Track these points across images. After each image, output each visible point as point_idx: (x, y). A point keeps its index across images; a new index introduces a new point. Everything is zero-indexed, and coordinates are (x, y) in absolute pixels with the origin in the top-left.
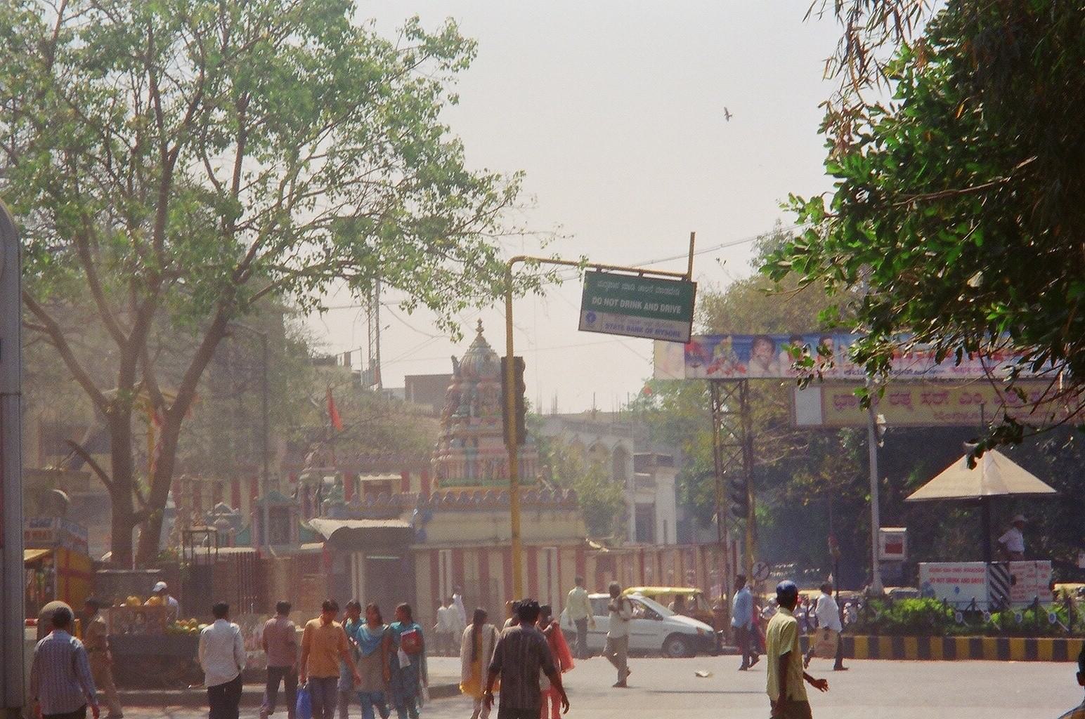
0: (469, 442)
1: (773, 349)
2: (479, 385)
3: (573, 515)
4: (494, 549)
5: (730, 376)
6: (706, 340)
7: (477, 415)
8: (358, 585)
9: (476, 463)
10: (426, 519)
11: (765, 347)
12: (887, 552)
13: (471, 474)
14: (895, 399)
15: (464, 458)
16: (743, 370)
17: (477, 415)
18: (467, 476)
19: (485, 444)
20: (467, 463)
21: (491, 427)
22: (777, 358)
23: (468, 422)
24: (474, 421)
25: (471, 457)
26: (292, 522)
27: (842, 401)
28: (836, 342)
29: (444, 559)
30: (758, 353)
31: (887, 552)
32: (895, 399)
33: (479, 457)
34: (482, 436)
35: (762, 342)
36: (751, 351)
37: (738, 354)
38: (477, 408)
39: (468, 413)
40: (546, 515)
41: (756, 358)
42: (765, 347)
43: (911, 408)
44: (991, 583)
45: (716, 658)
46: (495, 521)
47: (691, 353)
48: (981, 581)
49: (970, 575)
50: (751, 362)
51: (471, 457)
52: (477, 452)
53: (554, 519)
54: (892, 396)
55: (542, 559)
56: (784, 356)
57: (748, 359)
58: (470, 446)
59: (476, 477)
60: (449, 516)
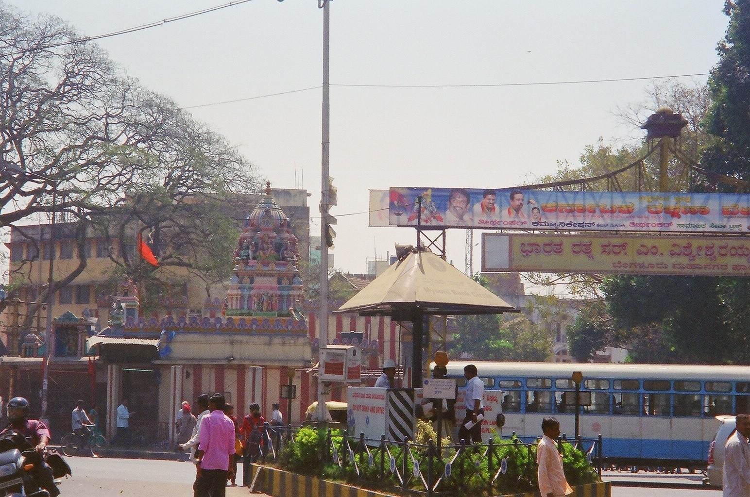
0: (247, 280)
1: (468, 201)
2: (259, 234)
3: (301, 340)
4: (231, 367)
5: (429, 224)
6: (409, 192)
7: (254, 258)
8: (111, 392)
9: (250, 296)
10: (170, 340)
11: (461, 199)
12: (326, 372)
13: (246, 307)
14: (577, 249)
15: (240, 292)
16: (441, 220)
17: (254, 258)
18: (242, 308)
19: (259, 281)
20: (242, 296)
21: (266, 268)
22: (471, 209)
23: (247, 264)
24: (251, 262)
25: (246, 292)
26: (80, 337)
27: (529, 248)
28: (526, 196)
29: (175, 372)
30: (454, 204)
31: (326, 372)
32: (577, 249)
33: (252, 292)
34: (257, 275)
35: (459, 195)
36: (448, 203)
37: (436, 204)
38: (255, 252)
39: (248, 256)
40: (277, 340)
41: (452, 208)
42: (461, 199)
43: (591, 257)
44: (391, 415)
45: (71, 469)
46: (232, 343)
47: (396, 203)
48: (379, 410)
49: (367, 402)
50: (448, 212)
51: (246, 292)
52: (252, 288)
53: (284, 344)
54: (574, 245)
55: (249, 375)
56: (477, 207)
57: (446, 209)
58: (246, 282)
59: (249, 308)
60: (191, 337)
